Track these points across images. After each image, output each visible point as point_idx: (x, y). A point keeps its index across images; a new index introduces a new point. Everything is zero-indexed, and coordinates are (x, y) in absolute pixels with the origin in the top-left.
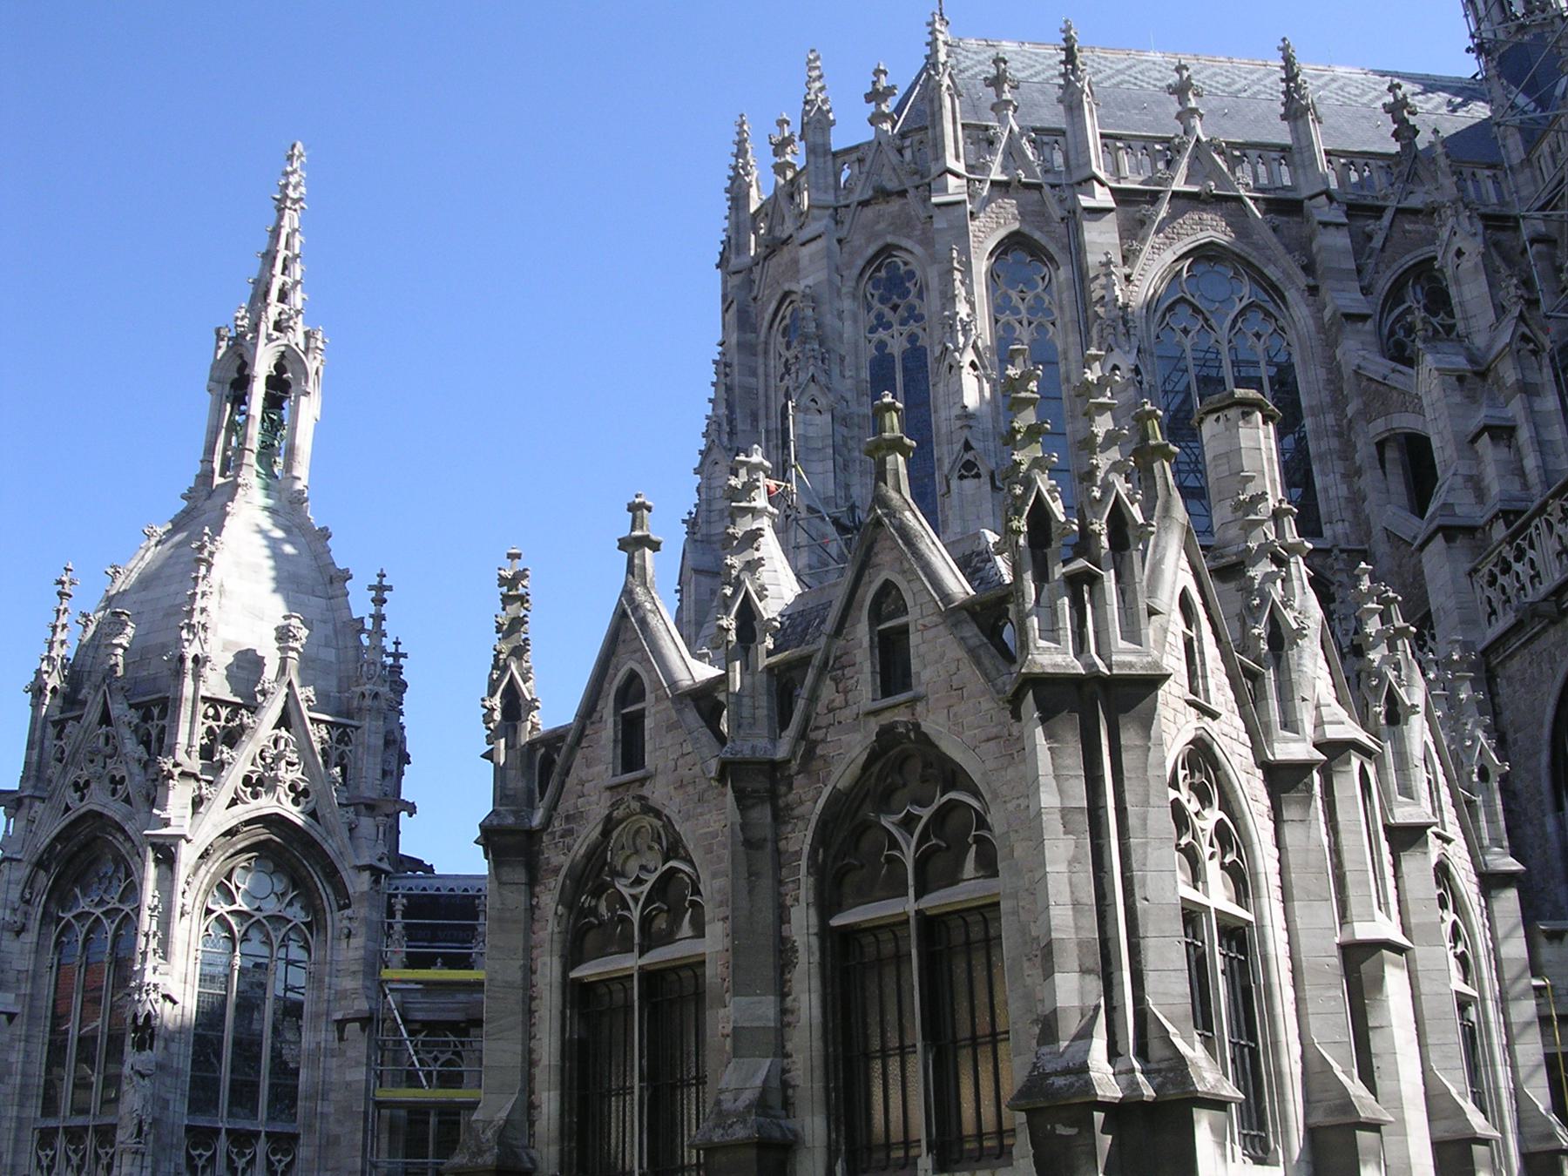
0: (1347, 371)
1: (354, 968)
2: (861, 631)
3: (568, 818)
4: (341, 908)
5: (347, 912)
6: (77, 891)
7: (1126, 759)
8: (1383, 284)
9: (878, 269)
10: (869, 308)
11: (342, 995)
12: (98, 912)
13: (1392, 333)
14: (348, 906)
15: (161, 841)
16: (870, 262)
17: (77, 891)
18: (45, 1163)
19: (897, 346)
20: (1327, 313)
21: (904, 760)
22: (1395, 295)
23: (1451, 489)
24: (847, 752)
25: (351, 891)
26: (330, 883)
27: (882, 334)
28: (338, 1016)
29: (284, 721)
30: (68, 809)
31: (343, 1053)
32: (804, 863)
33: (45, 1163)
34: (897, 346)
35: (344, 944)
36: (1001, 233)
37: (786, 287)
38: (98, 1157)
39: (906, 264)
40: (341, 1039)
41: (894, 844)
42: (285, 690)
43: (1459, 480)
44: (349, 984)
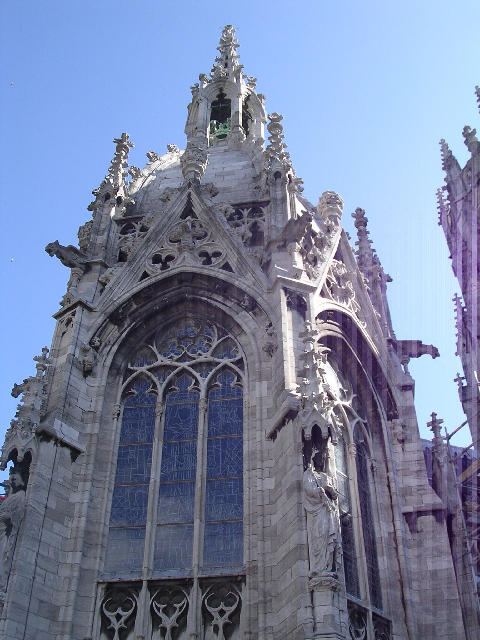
1: (413, 468)
4: (390, 418)
5: (398, 421)
6: (154, 348)
11: (407, 492)
12: (185, 365)
14: (396, 416)
15: (292, 288)
17: (154, 348)
18: (116, 625)
25: (398, 404)
26: (380, 395)
28: (409, 509)
29: (338, 256)
30: (145, 275)
31: (420, 544)
33: (116, 625)
35: (398, 447)
38: (207, 617)
40: (414, 531)
42: (340, 237)
44: (411, 481)
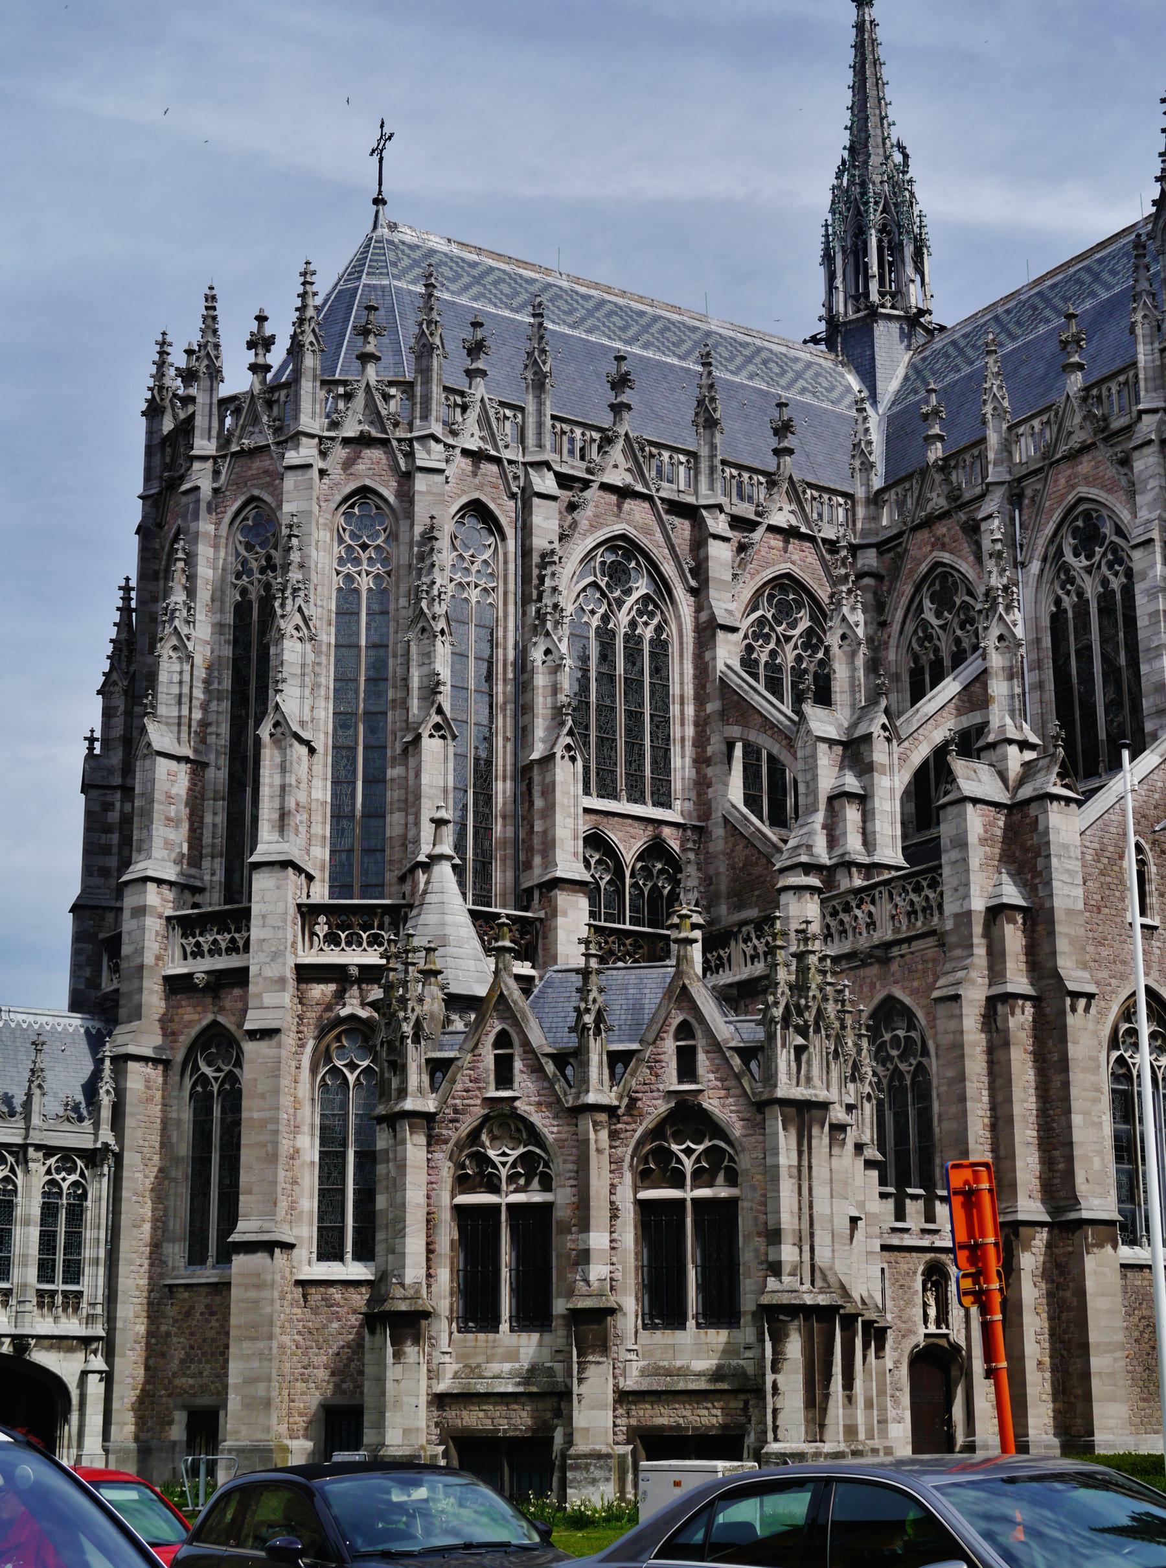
2: (670, 1046)
3: (456, 1111)
7: (814, 1142)
8: (747, 594)
9: (352, 506)
10: (341, 540)
16: (345, 500)
19: (365, 583)
20: (704, 616)
21: (688, 1117)
24: (656, 1108)
27: (349, 568)
32: (626, 1164)
34: (365, 583)
36: (464, 500)
37: (256, 493)
39: (378, 508)
41: (679, 1161)
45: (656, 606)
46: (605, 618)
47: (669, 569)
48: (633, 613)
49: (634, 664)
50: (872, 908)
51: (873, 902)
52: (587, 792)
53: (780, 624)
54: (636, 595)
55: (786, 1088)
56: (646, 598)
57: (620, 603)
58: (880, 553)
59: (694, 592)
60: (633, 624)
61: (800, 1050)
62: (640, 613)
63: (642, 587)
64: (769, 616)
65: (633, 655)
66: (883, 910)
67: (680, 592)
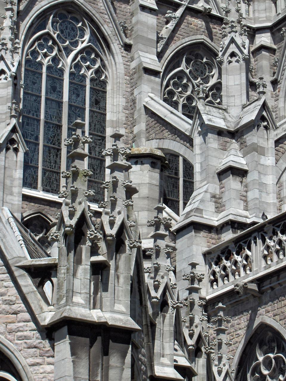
0: (139, 106)
8: (169, 53)
13: (167, 85)
20: (133, 65)
22: (174, 62)
23: (202, 201)
43: (208, 196)
45: (97, 55)
46: (55, 60)
47: (108, 29)
48: (79, 58)
49: (78, 95)
50: (249, 253)
51: (249, 249)
52: (29, 181)
53: (196, 78)
54: (80, 46)
55: (81, 310)
56: (87, 50)
57: (68, 51)
58: (273, 35)
59: (128, 47)
60: (78, 66)
61: (99, 270)
62: (84, 59)
63: (85, 42)
64: (187, 71)
65: (77, 87)
66: (257, 250)
67: (116, 47)
